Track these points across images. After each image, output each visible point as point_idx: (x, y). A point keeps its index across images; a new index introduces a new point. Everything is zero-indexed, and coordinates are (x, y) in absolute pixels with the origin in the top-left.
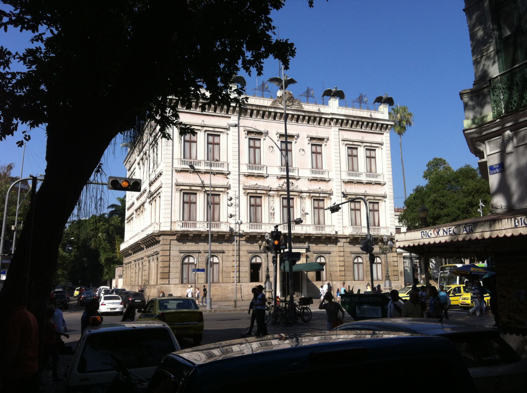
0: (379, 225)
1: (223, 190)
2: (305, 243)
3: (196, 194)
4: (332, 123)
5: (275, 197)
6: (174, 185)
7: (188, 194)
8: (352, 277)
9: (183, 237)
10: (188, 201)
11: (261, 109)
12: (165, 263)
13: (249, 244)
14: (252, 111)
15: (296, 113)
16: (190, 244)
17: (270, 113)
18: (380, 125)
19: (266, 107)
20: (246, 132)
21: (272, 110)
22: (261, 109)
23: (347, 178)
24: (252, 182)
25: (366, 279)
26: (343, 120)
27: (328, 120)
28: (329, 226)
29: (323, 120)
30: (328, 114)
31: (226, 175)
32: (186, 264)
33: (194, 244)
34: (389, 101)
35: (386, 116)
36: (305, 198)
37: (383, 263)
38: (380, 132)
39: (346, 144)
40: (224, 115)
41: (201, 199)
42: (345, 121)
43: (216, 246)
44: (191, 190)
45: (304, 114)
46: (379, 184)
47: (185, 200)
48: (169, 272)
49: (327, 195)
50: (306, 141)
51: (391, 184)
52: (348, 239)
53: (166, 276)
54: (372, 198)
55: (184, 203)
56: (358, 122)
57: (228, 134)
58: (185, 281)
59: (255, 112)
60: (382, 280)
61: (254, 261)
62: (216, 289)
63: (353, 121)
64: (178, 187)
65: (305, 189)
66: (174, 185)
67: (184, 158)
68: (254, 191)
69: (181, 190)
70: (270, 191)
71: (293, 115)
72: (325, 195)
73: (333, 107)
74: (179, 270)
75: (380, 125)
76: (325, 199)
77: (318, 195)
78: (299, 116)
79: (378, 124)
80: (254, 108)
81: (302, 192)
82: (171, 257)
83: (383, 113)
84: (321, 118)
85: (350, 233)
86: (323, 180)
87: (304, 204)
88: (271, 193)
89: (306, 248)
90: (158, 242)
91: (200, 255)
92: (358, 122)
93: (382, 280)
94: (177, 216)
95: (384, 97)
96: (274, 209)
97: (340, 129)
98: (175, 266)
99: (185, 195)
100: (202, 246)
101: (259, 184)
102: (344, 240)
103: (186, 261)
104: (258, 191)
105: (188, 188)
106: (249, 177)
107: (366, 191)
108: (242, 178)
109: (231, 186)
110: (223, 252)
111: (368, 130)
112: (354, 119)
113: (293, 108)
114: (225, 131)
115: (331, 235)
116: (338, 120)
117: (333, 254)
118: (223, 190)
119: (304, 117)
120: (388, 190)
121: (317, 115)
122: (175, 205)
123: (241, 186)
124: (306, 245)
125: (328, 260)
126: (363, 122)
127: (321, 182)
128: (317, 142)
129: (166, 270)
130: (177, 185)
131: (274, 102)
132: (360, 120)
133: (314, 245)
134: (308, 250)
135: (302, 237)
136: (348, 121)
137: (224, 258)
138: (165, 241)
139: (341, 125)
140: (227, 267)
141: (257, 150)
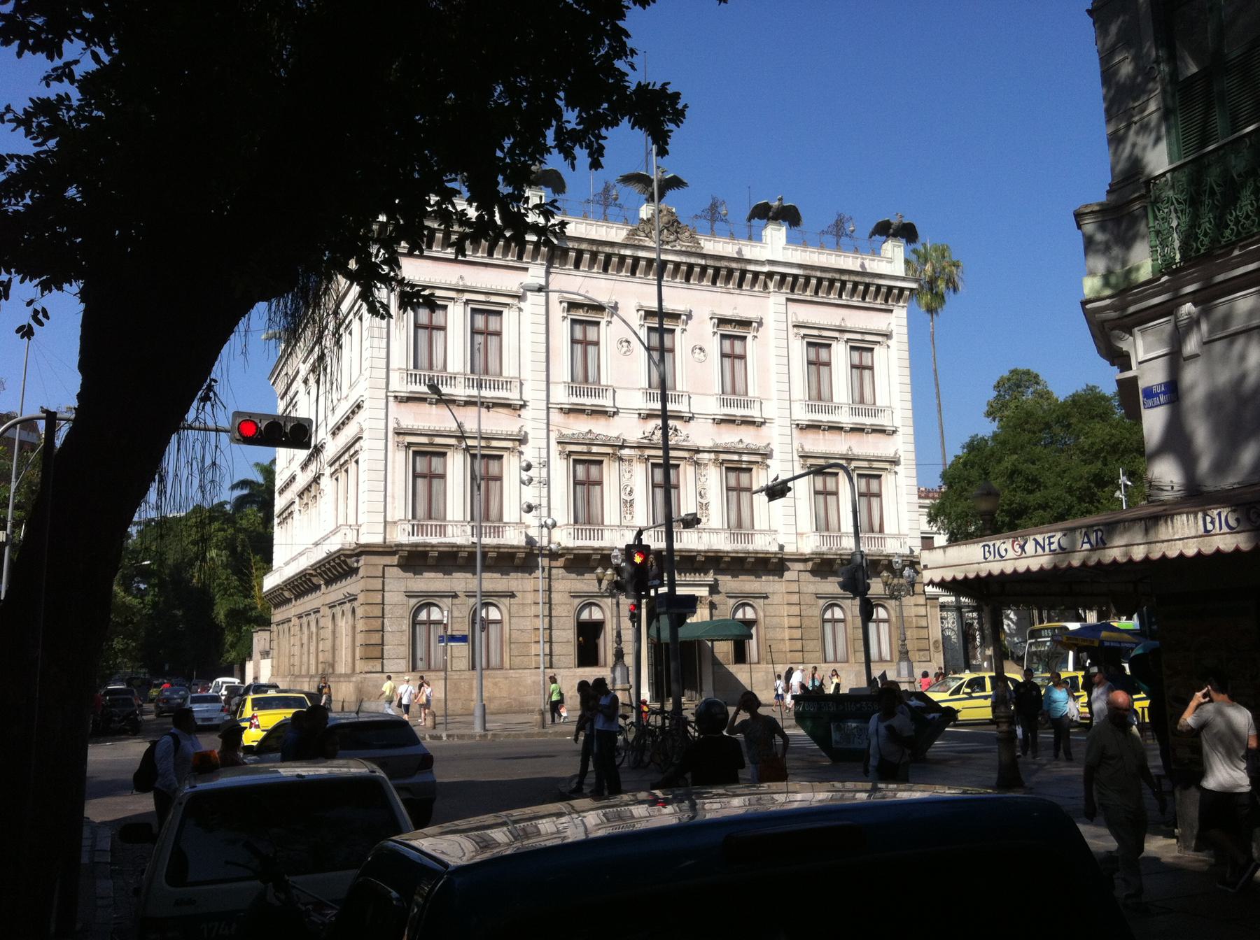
0: (881, 530)
1: (509, 444)
2: (706, 573)
3: (444, 454)
4: (771, 285)
5: (634, 463)
6: (390, 434)
7: (425, 455)
8: (819, 654)
9: (415, 559)
10: (426, 471)
11: (600, 249)
12: (372, 621)
13: (573, 576)
14: (580, 253)
15: (684, 259)
16: (432, 575)
17: (623, 258)
18: (884, 290)
19: (612, 244)
20: (565, 305)
21: (628, 252)
22: (600, 249)
23: (805, 417)
24: (580, 426)
25: (852, 660)
26: (796, 277)
27: (762, 277)
28: (762, 532)
29: (749, 276)
30: (762, 263)
31: (516, 408)
32: (423, 623)
33: (441, 575)
34: (907, 233)
35: (899, 269)
36: (706, 465)
37: (894, 619)
38: (883, 307)
39: (804, 336)
40: (511, 264)
41: (456, 468)
42: (801, 280)
43: (493, 582)
44: (431, 444)
45: (703, 262)
46: (883, 431)
47: (418, 470)
48: (383, 644)
49: (758, 458)
50: (709, 327)
51: (910, 430)
52: (810, 564)
53: (375, 652)
54: (865, 464)
55: (415, 476)
56: (832, 282)
57: (520, 310)
58: (420, 664)
59: (587, 256)
60: (891, 661)
61: (585, 615)
62: (495, 684)
63: (820, 280)
64: (401, 438)
65: (705, 443)
66: (390, 434)
67: (416, 367)
68: (584, 449)
69: (409, 445)
70: (622, 447)
71: (677, 265)
72: (753, 458)
73: (774, 246)
74: (406, 638)
75: (884, 290)
76: (755, 468)
77: (736, 457)
78: (691, 267)
79: (879, 287)
80: (584, 246)
81: (698, 451)
82: (387, 608)
83: (891, 261)
84: (743, 273)
85: (815, 550)
86: (747, 422)
87: (703, 479)
88: (626, 452)
89: (710, 586)
90: (355, 571)
91: (456, 601)
92: (832, 282)
93: (891, 661)
94: (399, 509)
95: (895, 221)
96: (631, 491)
97: (788, 300)
98: (395, 628)
99: (418, 458)
100: (460, 581)
101: (596, 430)
102: (800, 566)
103: (423, 616)
104: (595, 449)
106: (572, 415)
107: (850, 449)
108: (556, 417)
109: (530, 437)
110: (512, 595)
111: (856, 301)
112: (824, 275)
113: (678, 248)
114: (515, 301)
115: (767, 553)
116: (784, 276)
117: (774, 599)
118: (509, 444)
119: (704, 269)
120: (902, 445)
121: (734, 265)
122: (393, 483)
123: (553, 436)
124: (710, 578)
125: (761, 614)
126: (844, 283)
127: (743, 427)
128: (734, 330)
129: (376, 638)
130: (398, 434)
131: (633, 233)
132: (837, 276)
133: (729, 578)
134: (714, 589)
135: (698, 558)
136: (808, 279)
137: (514, 609)
138: (370, 568)
139: (792, 290)
140: (522, 631)
141: (591, 349)
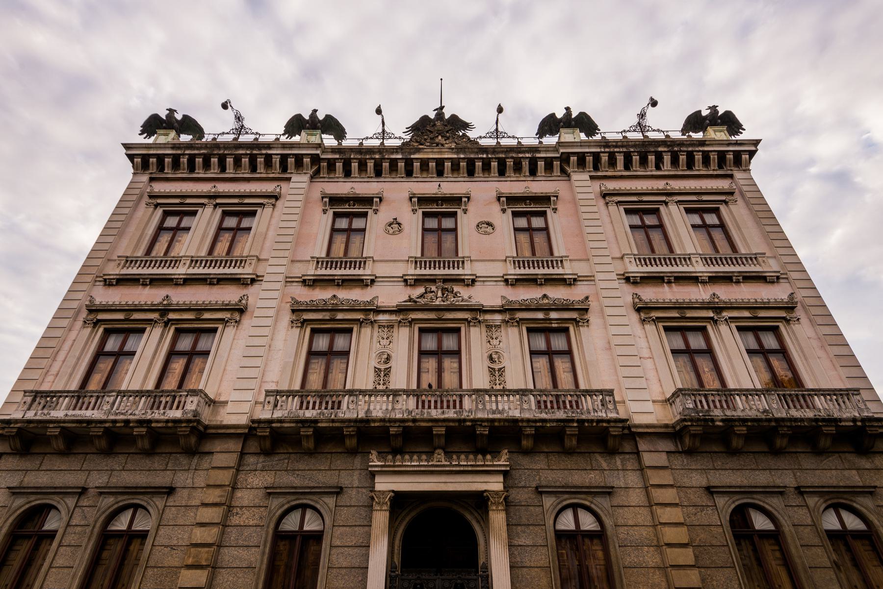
1: (226, 315)
2: (496, 454)
20: (327, 200)
27: (556, 164)
49: (574, 315)
54: (746, 314)
61: (291, 524)
70: (378, 311)
77: (540, 315)
87: (495, 342)
88: (381, 317)
96: (388, 359)
97: (592, 178)
104: (340, 316)
105: (120, 316)
124: (503, 461)
125: (608, 522)
135: (479, 430)
